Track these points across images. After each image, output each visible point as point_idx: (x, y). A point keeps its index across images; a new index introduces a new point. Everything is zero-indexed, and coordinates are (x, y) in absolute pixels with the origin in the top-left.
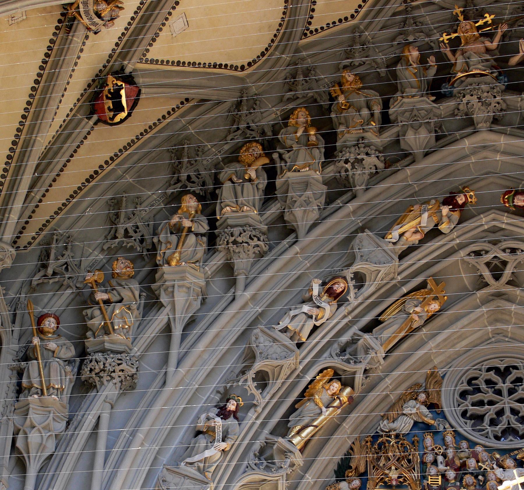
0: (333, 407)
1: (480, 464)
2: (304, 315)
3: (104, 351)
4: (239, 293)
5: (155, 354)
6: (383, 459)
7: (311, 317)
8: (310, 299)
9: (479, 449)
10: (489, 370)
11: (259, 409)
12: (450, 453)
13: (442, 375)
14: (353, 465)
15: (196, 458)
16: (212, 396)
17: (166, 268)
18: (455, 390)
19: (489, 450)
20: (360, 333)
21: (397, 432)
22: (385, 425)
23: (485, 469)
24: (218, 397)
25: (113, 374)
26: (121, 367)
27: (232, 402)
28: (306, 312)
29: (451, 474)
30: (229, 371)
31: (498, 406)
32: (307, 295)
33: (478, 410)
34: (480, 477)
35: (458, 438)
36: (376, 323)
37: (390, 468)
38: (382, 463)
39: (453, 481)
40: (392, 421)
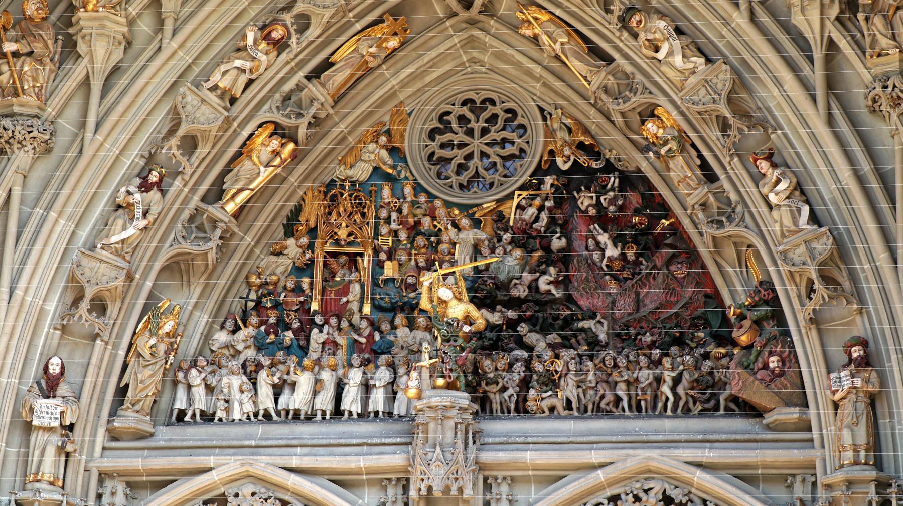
0: (273, 166)
1: (435, 223)
2: (236, 71)
3: (11, 115)
4: (165, 41)
5: (73, 112)
6: (334, 213)
7: (244, 71)
8: (245, 48)
9: (438, 203)
10: (464, 103)
11: (187, 178)
12: (405, 211)
13: (409, 111)
14: (302, 219)
15: (114, 239)
16: (136, 160)
17: (81, 13)
18: (422, 129)
19: (448, 205)
20: (305, 81)
21: (354, 179)
22: (341, 172)
23: (440, 230)
24: (142, 163)
25: (24, 143)
26: (31, 135)
27: (154, 173)
28: (239, 66)
29: (403, 236)
30: (156, 131)
31: (466, 151)
32: (242, 44)
33: (447, 153)
34: (432, 239)
35: (418, 189)
36: (327, 64)
37: (341, 225)
38: (334, 216)
39: (405, 242)
40: (349, 166)
